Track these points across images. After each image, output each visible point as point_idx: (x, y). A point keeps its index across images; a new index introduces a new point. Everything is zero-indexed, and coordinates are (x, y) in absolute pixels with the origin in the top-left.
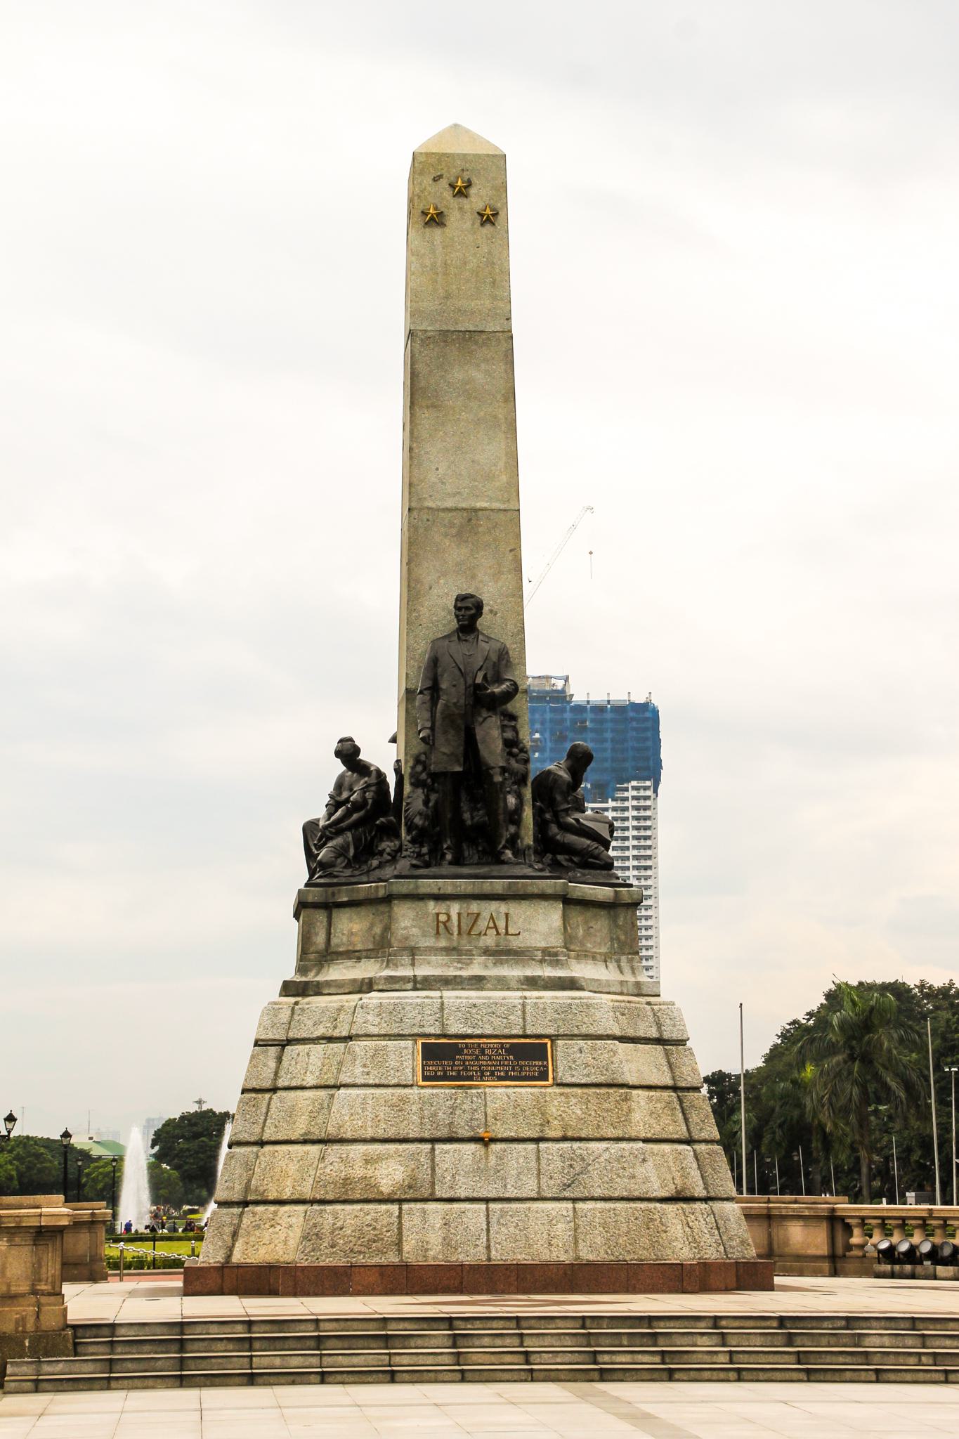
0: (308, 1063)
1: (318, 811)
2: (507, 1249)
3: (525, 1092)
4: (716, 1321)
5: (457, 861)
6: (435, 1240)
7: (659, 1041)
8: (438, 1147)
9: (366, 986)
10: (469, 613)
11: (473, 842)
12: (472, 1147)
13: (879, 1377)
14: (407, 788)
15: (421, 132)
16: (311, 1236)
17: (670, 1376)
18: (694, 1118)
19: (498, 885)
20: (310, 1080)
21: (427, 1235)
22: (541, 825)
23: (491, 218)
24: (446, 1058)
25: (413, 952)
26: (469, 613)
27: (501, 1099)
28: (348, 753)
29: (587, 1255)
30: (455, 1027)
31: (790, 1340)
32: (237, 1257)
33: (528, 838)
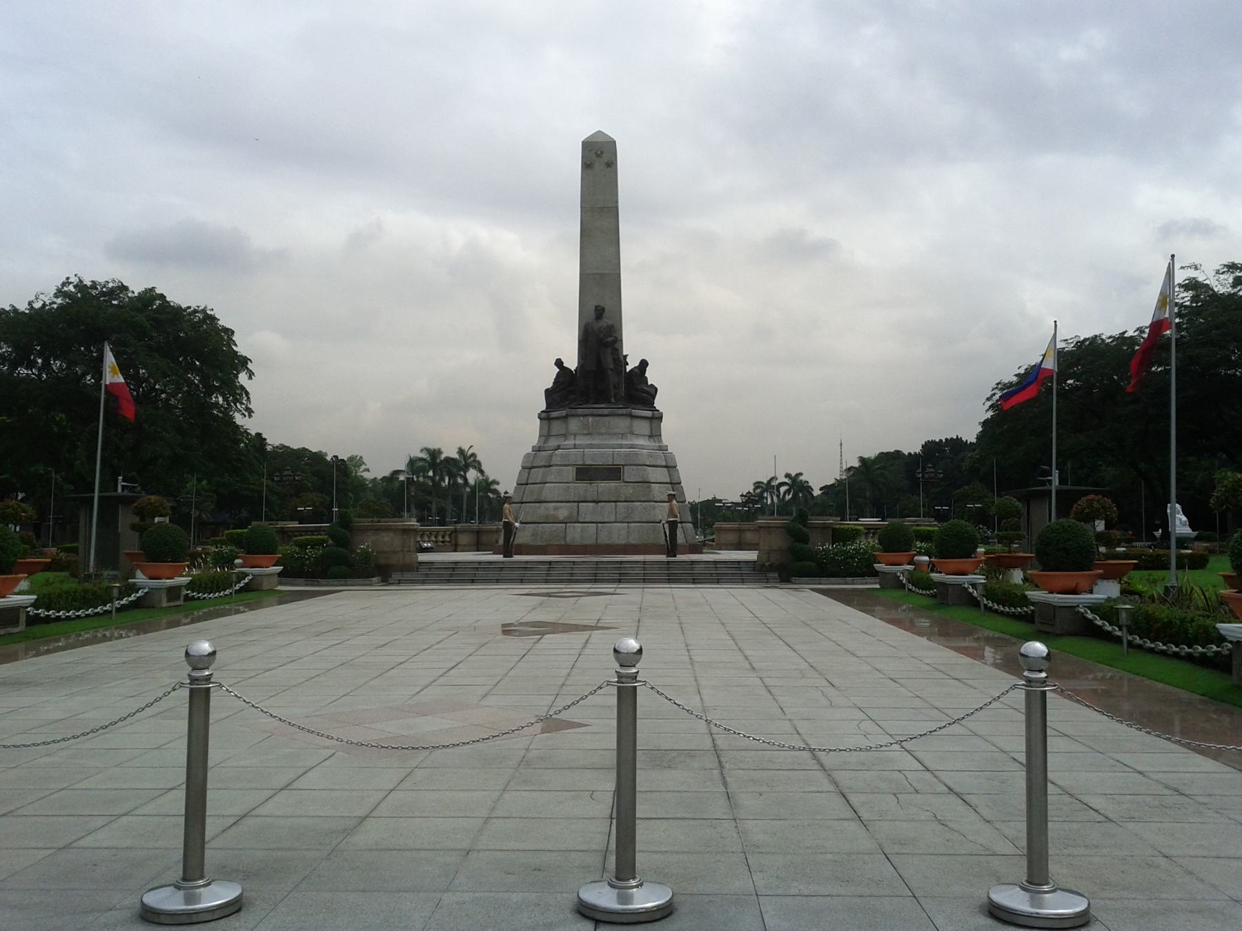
0: (537, 475)
1: (550, 385)
2: (604, 539)
3: (613, 484)
4: (644, 562)
6: (577, 536)
9: (558, 448)
10: (600, 312)
13: (694, 582)
15: (587, 133)
16: (534, 535)
17: (620, 581)
19: (606, 411)
21: (575, 534)
23: (612, 164)
24: (586, 473)
25: (575, 435)
26: (600, 312)
27: (604, 486)
28: (559, 363)
30: (588, 462)
31: (668, 569)
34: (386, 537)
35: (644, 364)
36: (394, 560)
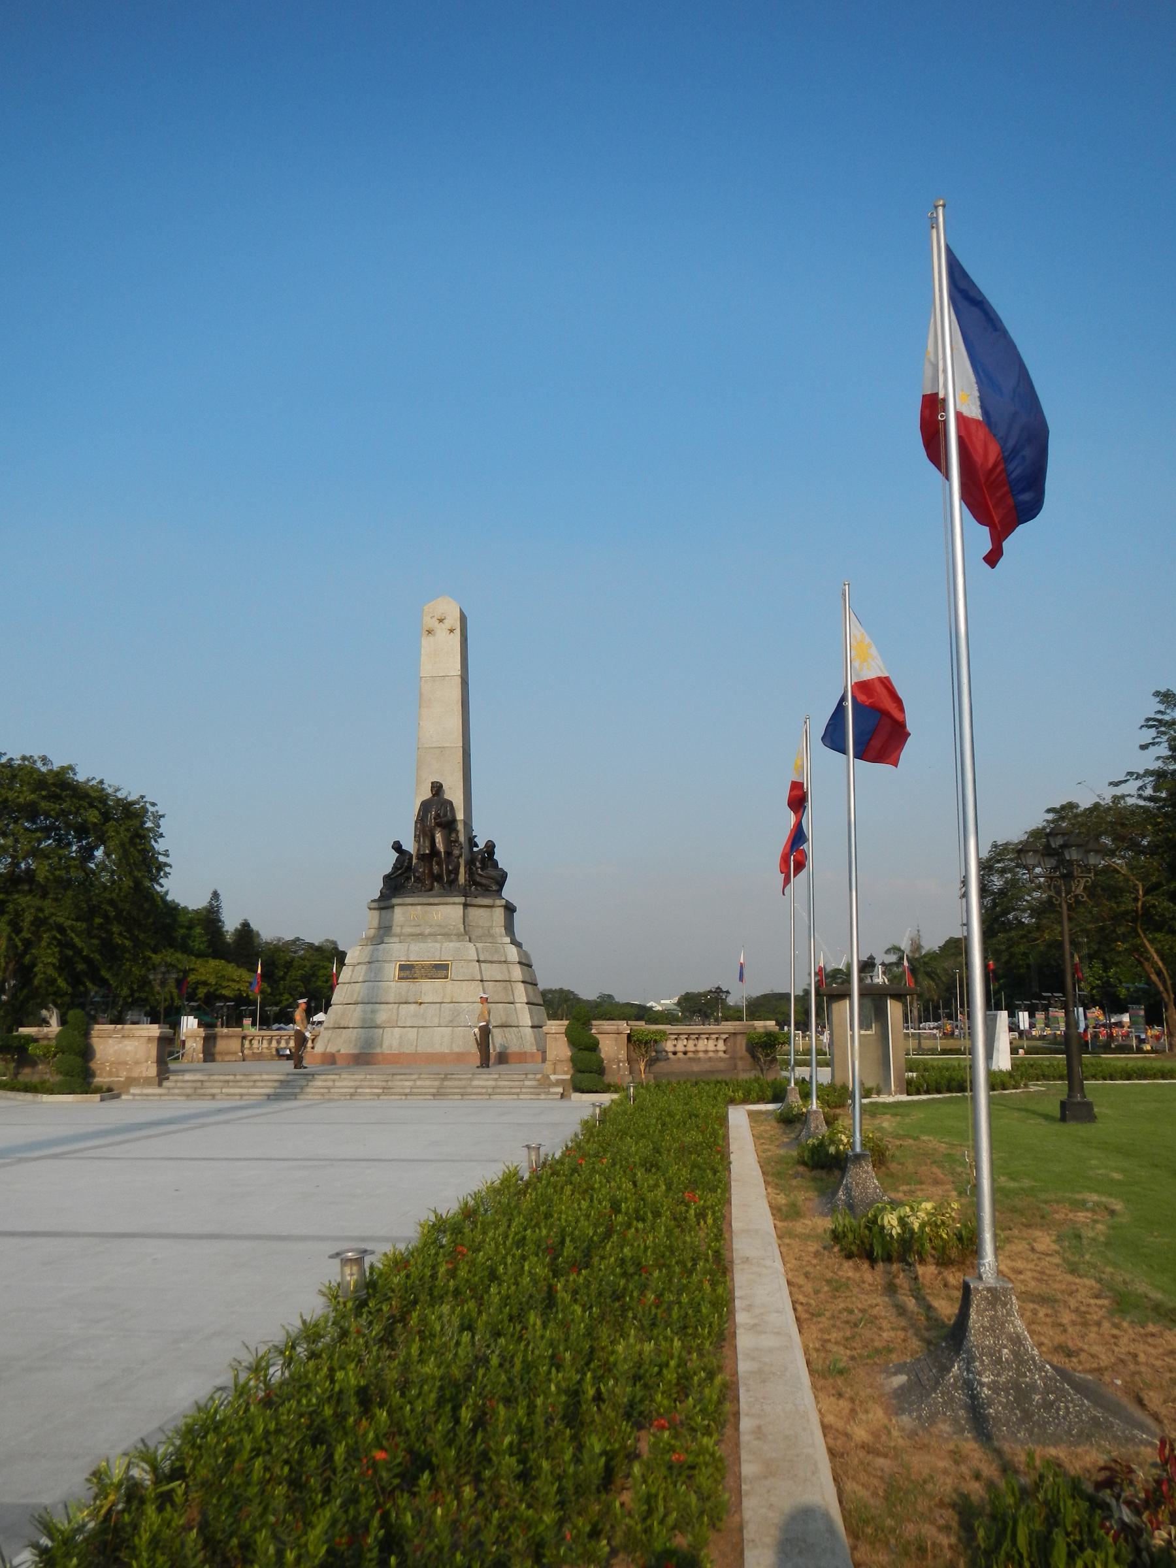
1: (388, 869)
5: (431, 890)
6: (395, 1043)
7: (505, 962)
8: (402, 1006)
11: (438, 882)
12: (413, 1007)
14: (414, 861)
18: (516, 994)
20: (360, 979)
22: (470, 872)
24: (408, 971)
28: (397, 847)
29: (456, 1049)
32: (328, 1050)
33: (462, 879)
34: (130, 1046)
35: (490, 847)
36: (135, 1074)
